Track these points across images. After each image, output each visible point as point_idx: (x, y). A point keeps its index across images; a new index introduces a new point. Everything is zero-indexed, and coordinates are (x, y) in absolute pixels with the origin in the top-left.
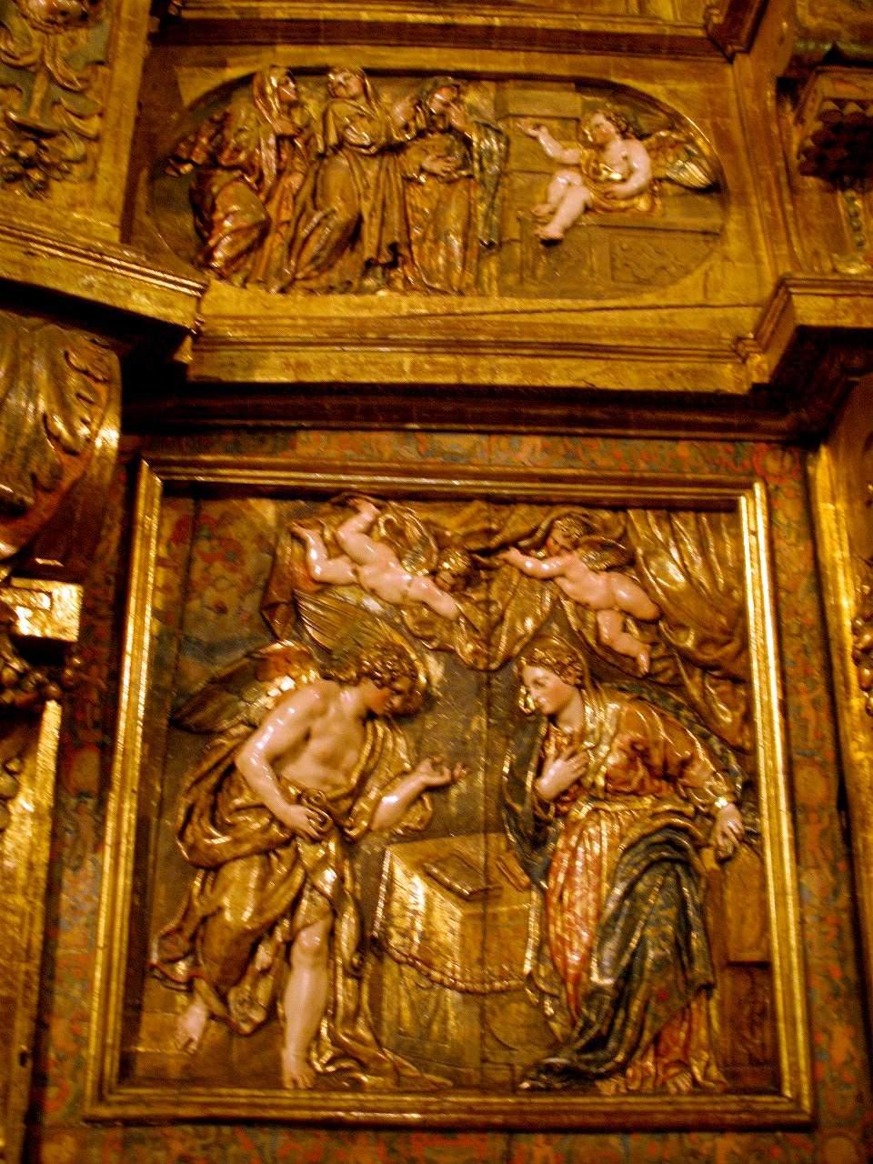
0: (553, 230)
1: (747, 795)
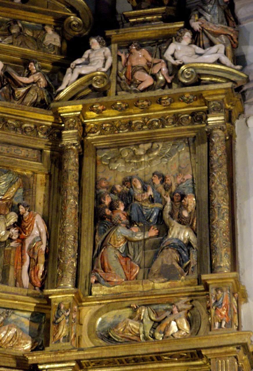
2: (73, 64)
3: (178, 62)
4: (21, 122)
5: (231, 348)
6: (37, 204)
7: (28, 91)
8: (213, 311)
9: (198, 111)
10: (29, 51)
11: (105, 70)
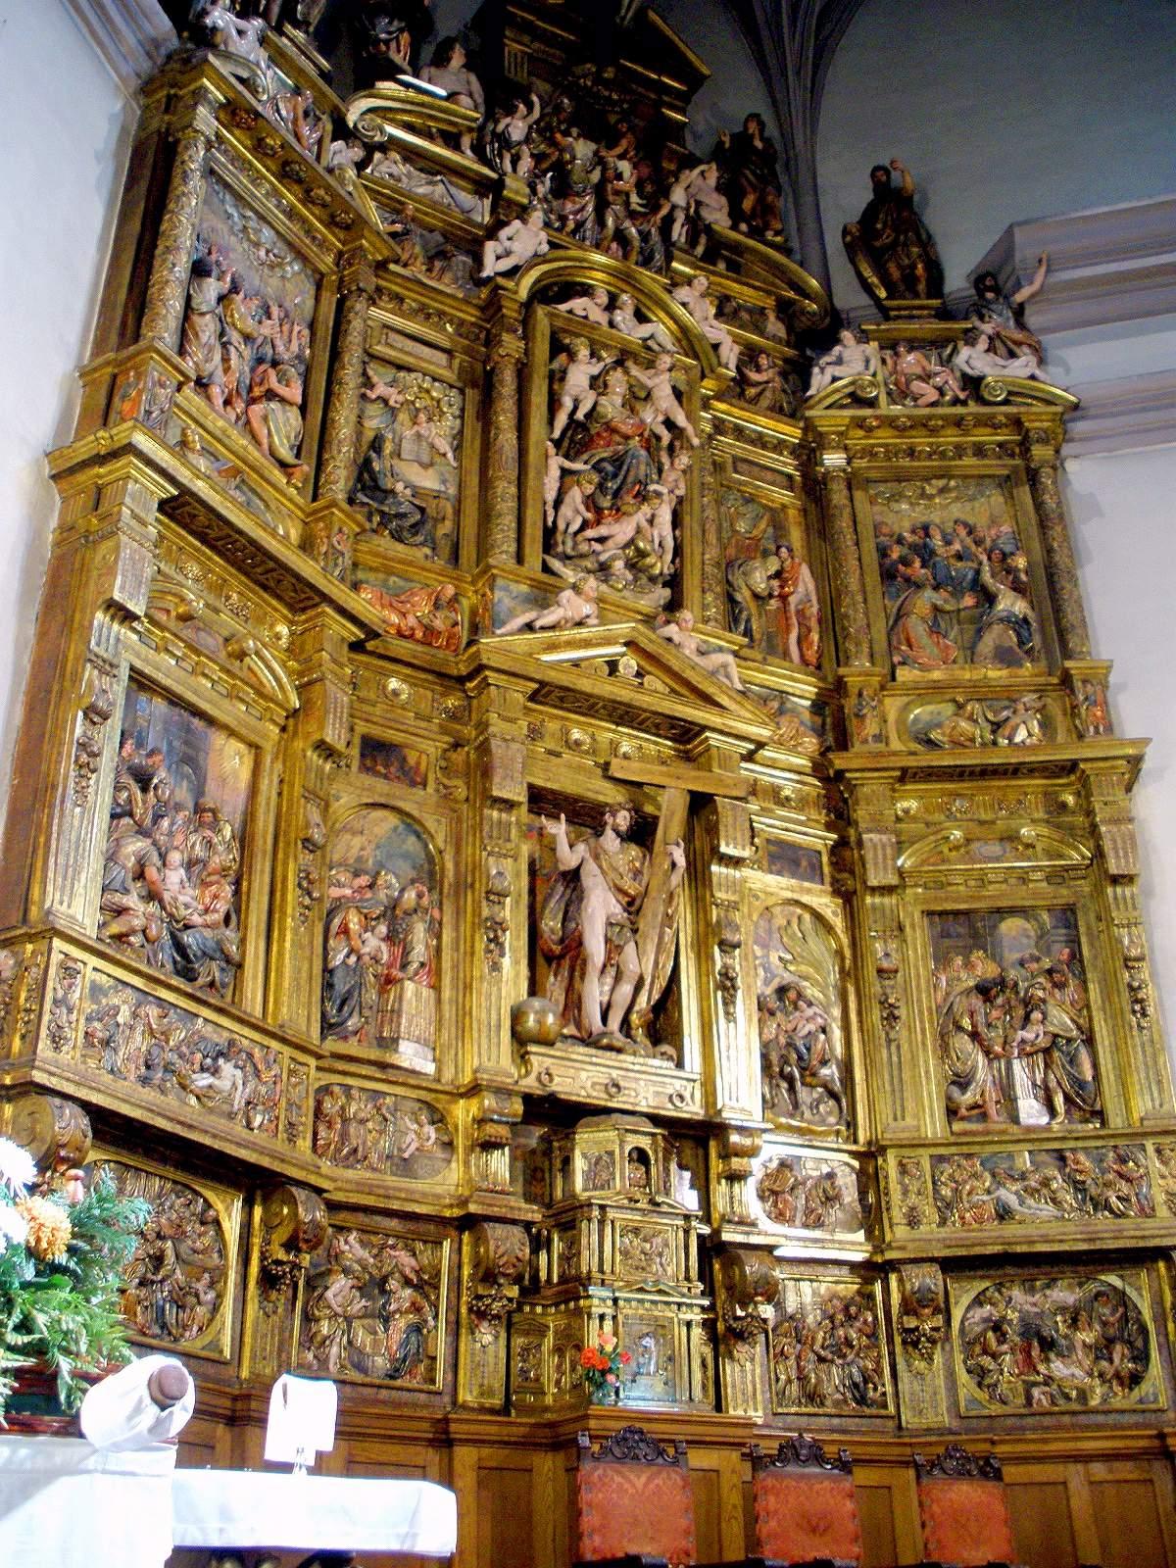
0: (406, 1155)
1: (436, 1317)
5: (1120, 762)
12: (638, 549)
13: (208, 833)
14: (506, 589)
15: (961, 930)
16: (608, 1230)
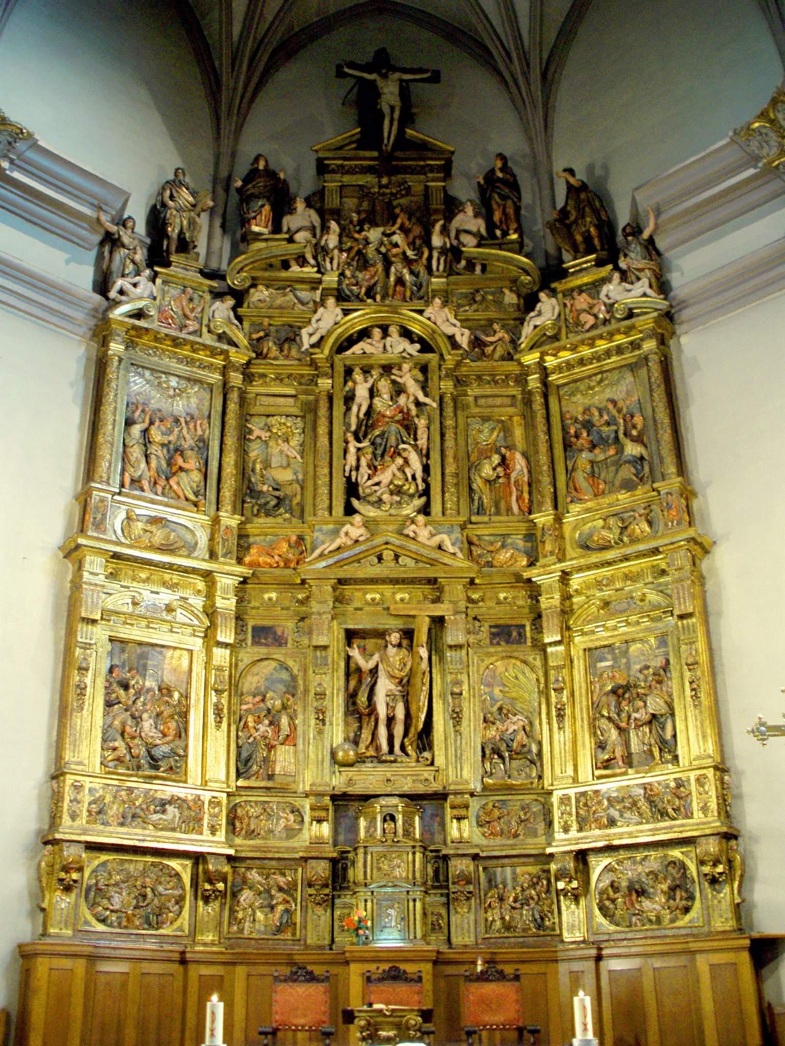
2: (528, 318)
3: (612, 301)
4: (494, 375)
5: (682, 543)
6: (517, 443)
7: (495, 348)
8: (665, 513)
9: (635, 340)
10: (492, 314)
11: (555, 317)
12: (395, 485)
13: (167, 698)
14: (320, 530)
15: (609, 657)
16: (369, 857)
